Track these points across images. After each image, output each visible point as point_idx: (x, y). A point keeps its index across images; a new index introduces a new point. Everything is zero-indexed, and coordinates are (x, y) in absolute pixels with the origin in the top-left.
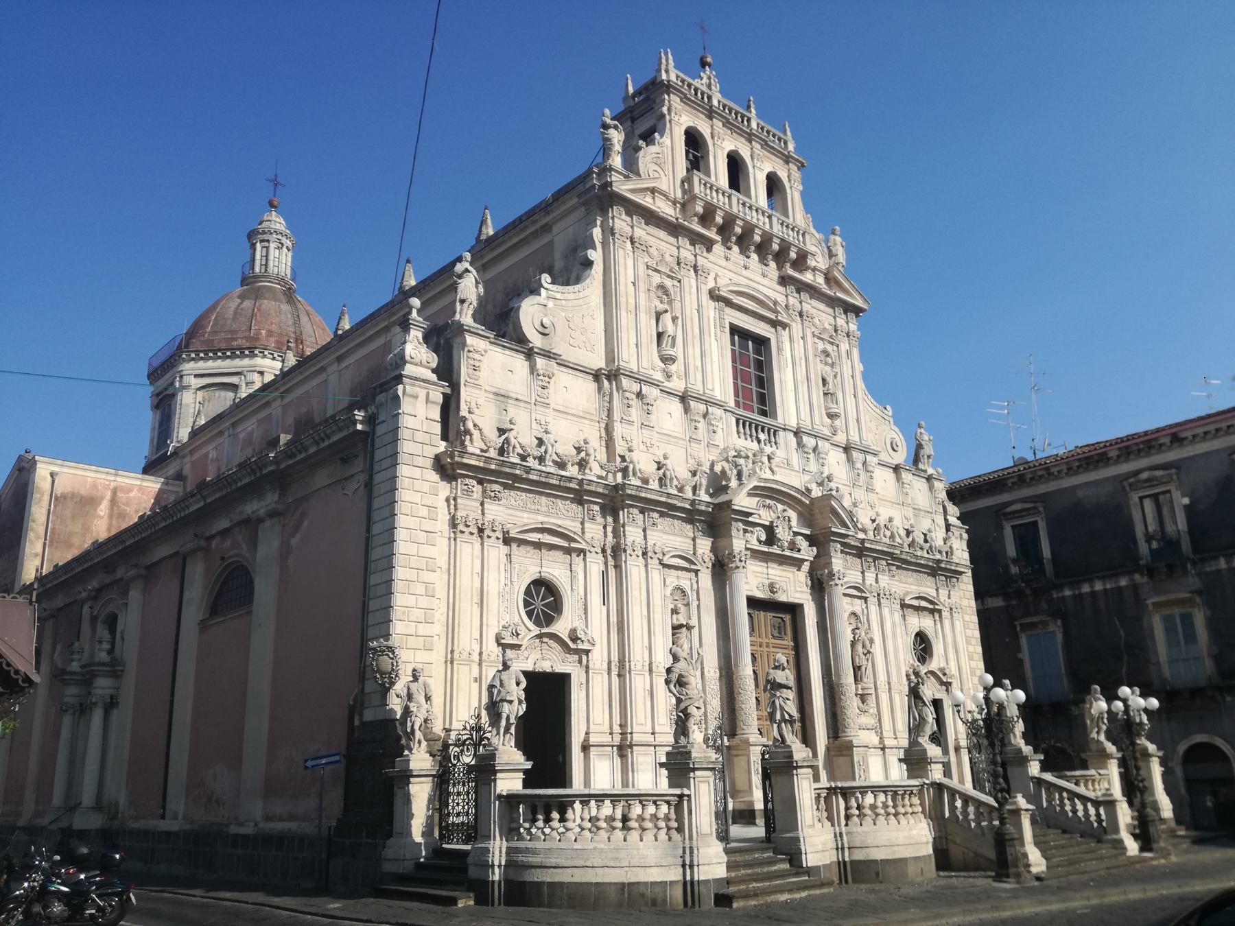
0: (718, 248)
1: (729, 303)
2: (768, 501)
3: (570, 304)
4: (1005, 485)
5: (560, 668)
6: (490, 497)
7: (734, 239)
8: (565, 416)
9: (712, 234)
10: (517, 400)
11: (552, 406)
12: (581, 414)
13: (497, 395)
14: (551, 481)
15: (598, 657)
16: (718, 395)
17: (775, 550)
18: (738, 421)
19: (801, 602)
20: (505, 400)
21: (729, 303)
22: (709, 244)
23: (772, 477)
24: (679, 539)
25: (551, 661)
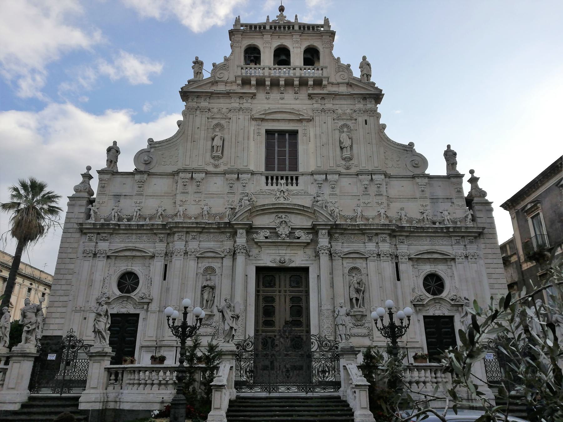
0: (261, 95)
1: (263, 120)
2: (280, 215)
3: (164, 147)
4: (557, 166)
5: (132, 311)
6: (101, 240)
7: (268, 88)
8: (152, 197)
9: (253, 90)
10: (125, 196)
11: (145, 194)
12: (163, 194)
13: (115, 195)
14: (133, 228)
15: (154, 306)
16: (252, 168)
17: (279, 240)
18: (267, 178)
19: (307, 265)
20: (119, 197)
21: (263, 120)
22: (253, 96)
23: (285, 202)
24: (213, 243)
25: (128, 309)
